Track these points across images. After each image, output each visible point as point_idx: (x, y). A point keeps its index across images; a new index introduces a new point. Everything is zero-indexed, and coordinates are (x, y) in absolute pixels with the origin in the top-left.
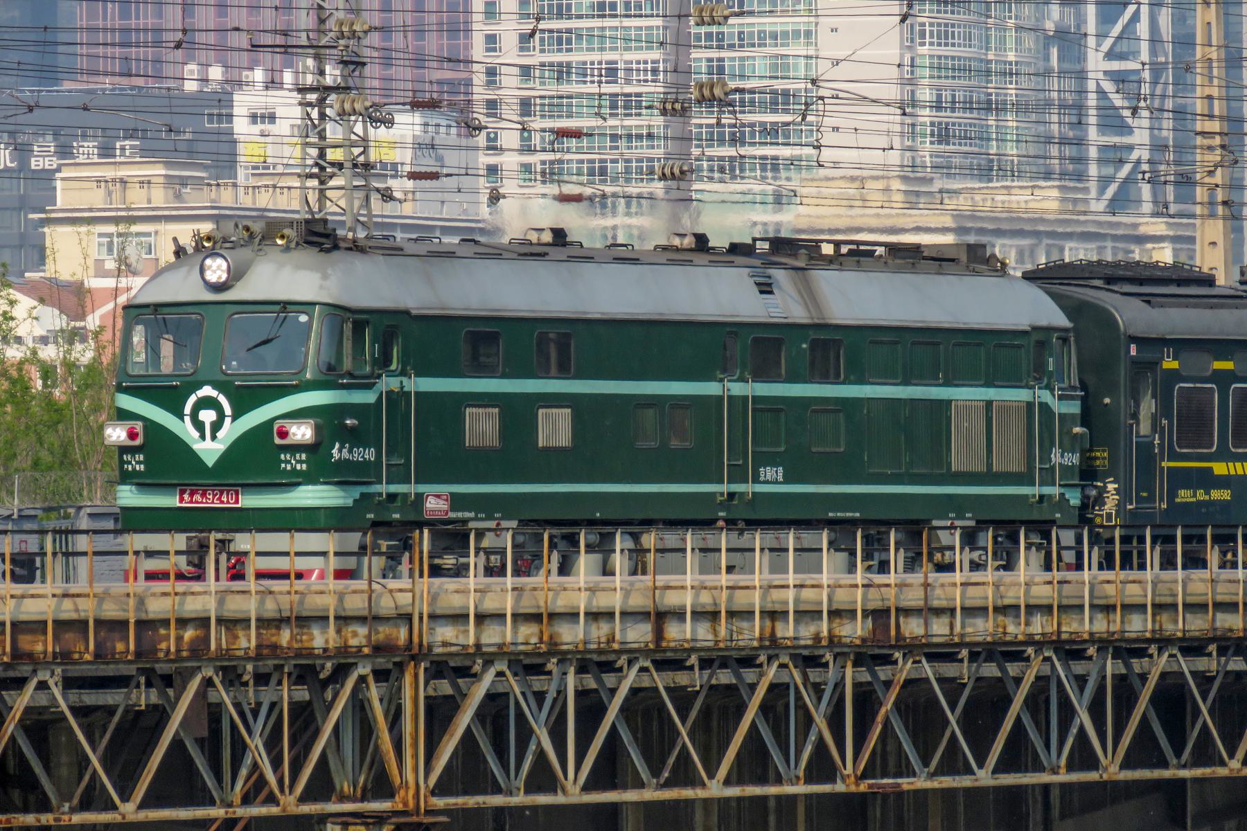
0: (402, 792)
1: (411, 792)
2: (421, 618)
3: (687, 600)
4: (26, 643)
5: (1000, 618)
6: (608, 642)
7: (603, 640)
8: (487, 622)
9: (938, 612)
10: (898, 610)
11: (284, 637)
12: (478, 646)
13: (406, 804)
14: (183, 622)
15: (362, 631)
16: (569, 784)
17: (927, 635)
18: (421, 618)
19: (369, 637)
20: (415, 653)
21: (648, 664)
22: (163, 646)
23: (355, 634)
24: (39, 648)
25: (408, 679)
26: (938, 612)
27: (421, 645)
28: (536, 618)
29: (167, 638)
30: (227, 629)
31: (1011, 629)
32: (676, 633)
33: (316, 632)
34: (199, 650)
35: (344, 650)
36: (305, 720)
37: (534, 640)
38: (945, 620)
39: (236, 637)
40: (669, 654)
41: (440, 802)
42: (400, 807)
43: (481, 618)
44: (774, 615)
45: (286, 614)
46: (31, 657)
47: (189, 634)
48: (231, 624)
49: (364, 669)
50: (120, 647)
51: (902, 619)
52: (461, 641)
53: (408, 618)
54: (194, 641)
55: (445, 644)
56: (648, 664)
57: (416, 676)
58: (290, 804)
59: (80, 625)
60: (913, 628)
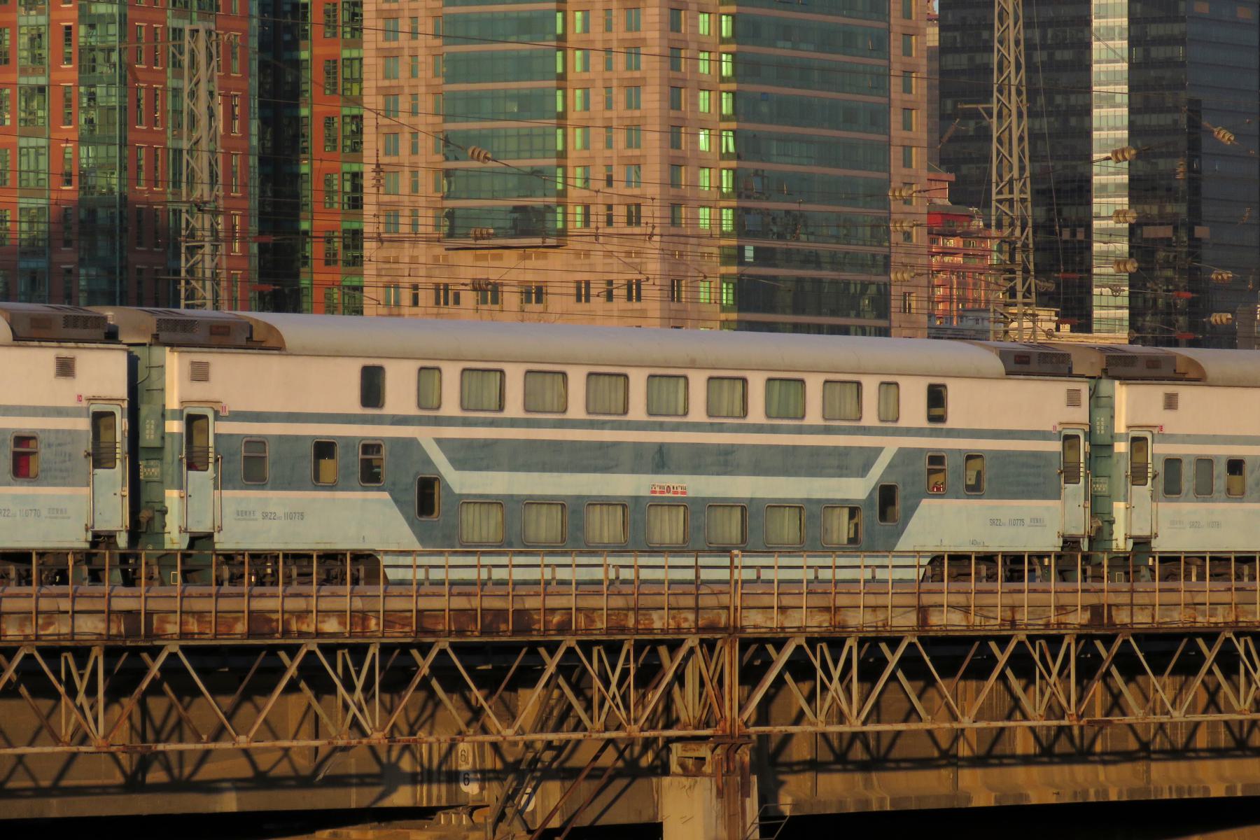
0: (722, 724)
1: (728, 724)
2: (736, 609)
3: (944, 599)
4: (428, 624)
5: (1190, 611)
6: (884, 626)
7: (880, 624)
8: (790, 611)
9: (1143, 607)
10: (1109, 606)
11: (631, 623)
12: (783, 628)
13: (724, 731)
14: (553, 610)
15: (691, 616)
16: (853, 719)
17: (1132, 623)
18: (736, 609)
19: (697, 620)
20: (732, 630)
21: (915, 640)
22: (536, 627)
23: (686, 620)
24: (440, 627)
25: (727, 649)
26: (1143, 607)
27: (735, 627)
28: (827, 609)
29: (539, 621)
30: (587, 617)
31: (1200, 619)
32: (936, 619)
33: (655, 615)
34: (564, 628)
35: (679, 629)
36: (648, 675)
37: (826, 624)
38: (1148, 612)
39: (593, 621)
40: (931, 634)
41: (752, 730)
42: (720, 733)
43: (783, 609)
44: (1013, 608)
45: (632, 604)
46: (433, 633)
47: (556, 619)
48: (590, 612)
49: (692, 641)
50: (503, 627)
51: (1114, 613)
52: (769, 624)
53: (728, 608)
54: (559, 623)
55: (755, 627)
56: (915, 640)
57: (732, 648)
58: (634, 730)
59: (468, 613)
60: (1122, 617)
